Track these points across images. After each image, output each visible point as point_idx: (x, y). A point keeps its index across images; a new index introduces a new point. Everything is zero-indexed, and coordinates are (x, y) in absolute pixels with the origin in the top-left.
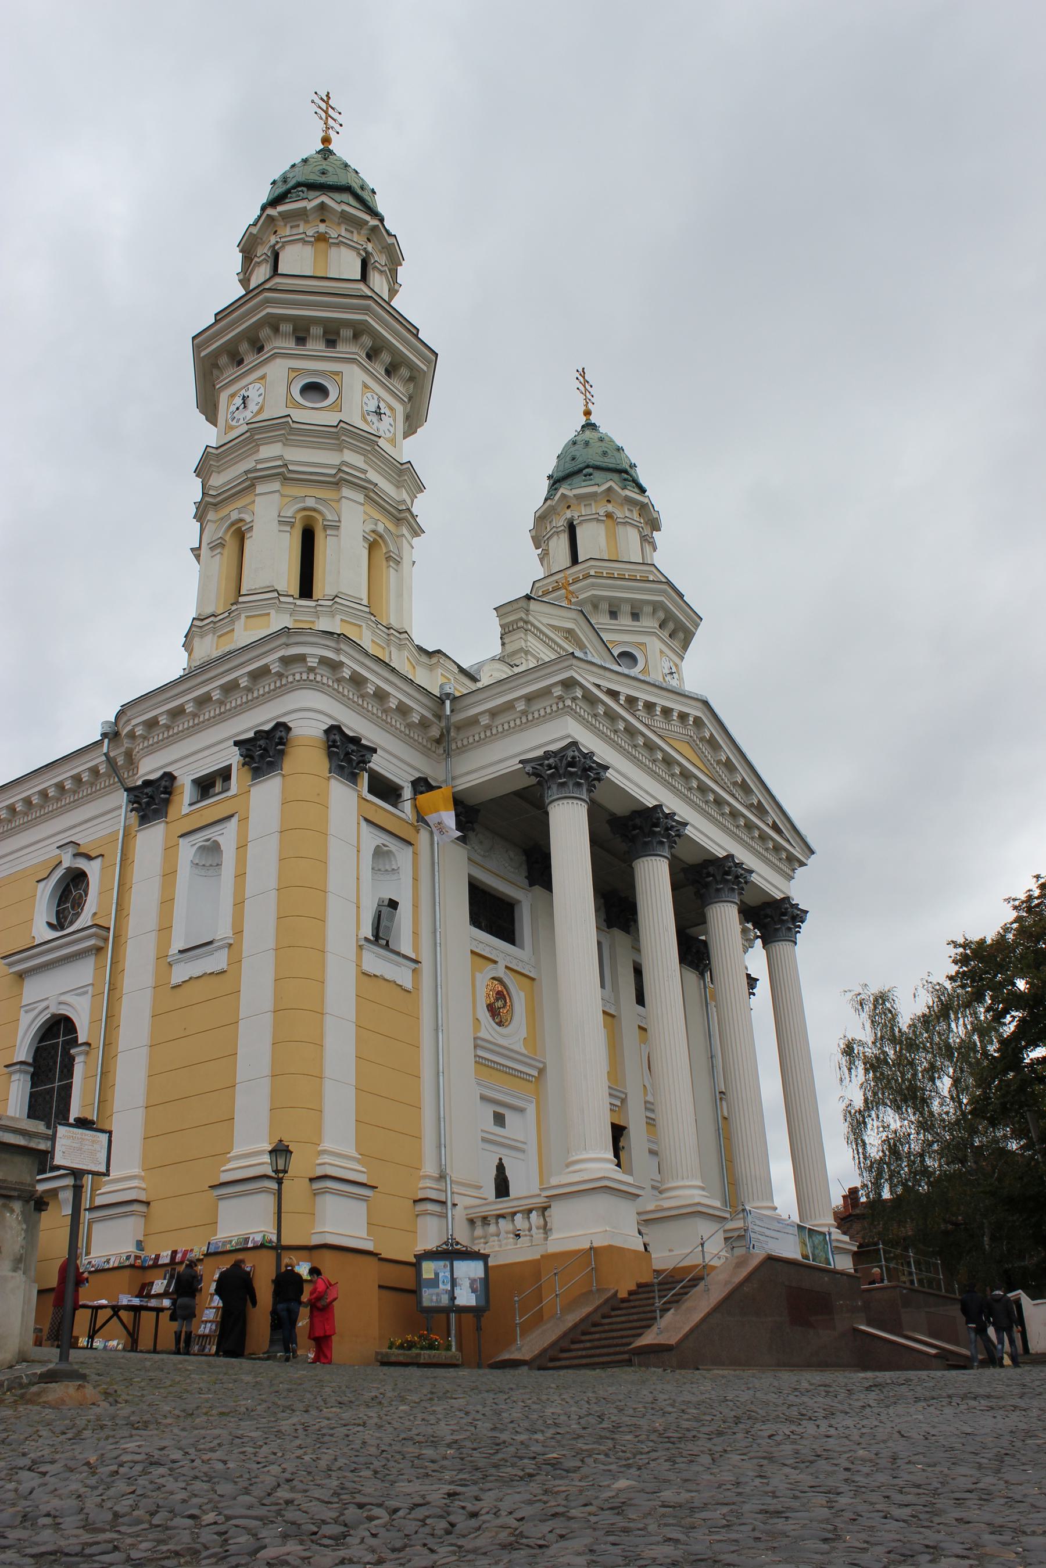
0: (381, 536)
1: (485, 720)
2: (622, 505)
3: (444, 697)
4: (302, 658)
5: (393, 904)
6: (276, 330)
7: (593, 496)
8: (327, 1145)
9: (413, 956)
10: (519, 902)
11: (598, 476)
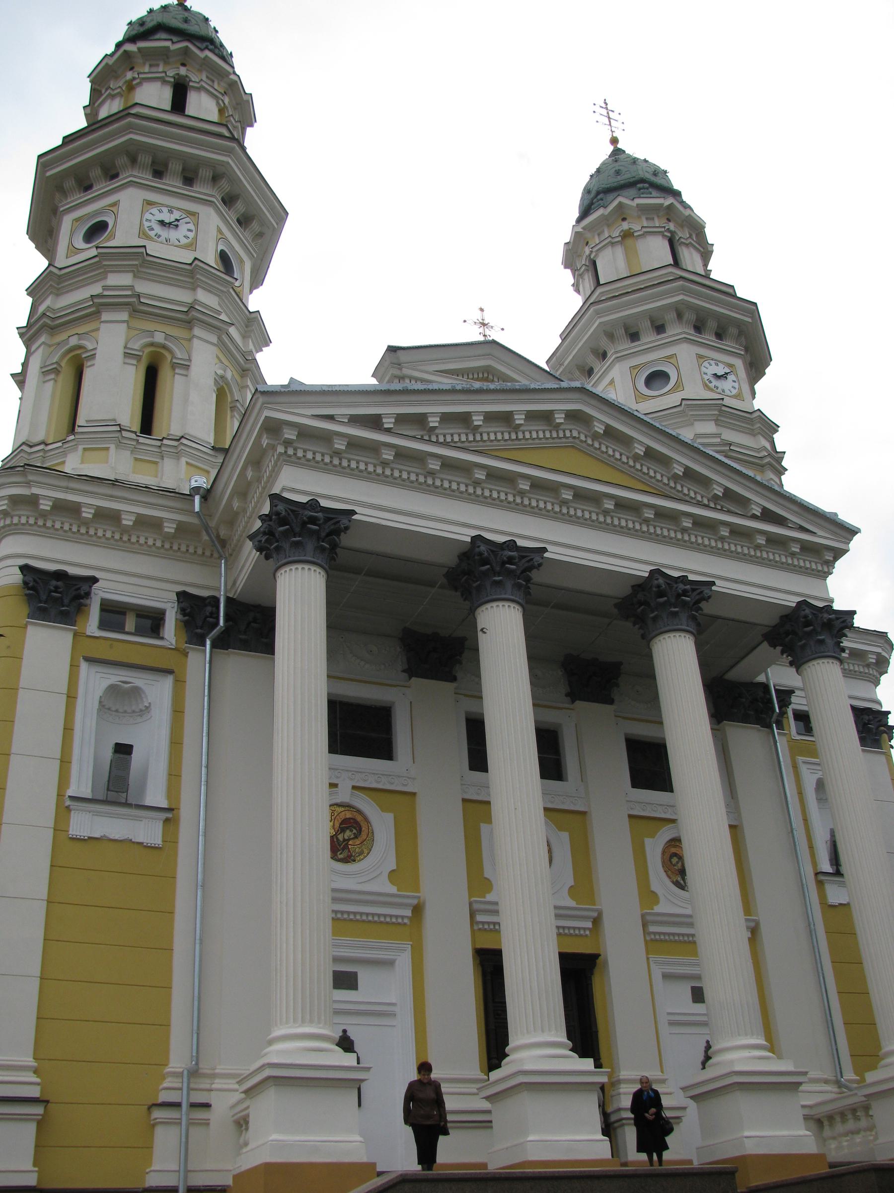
0: (164, 347)
1: (236, 504)
2: (639, 217)
3: (193, 493)
9: (164, 804)
10: (394, 703)
11: (611, 196)
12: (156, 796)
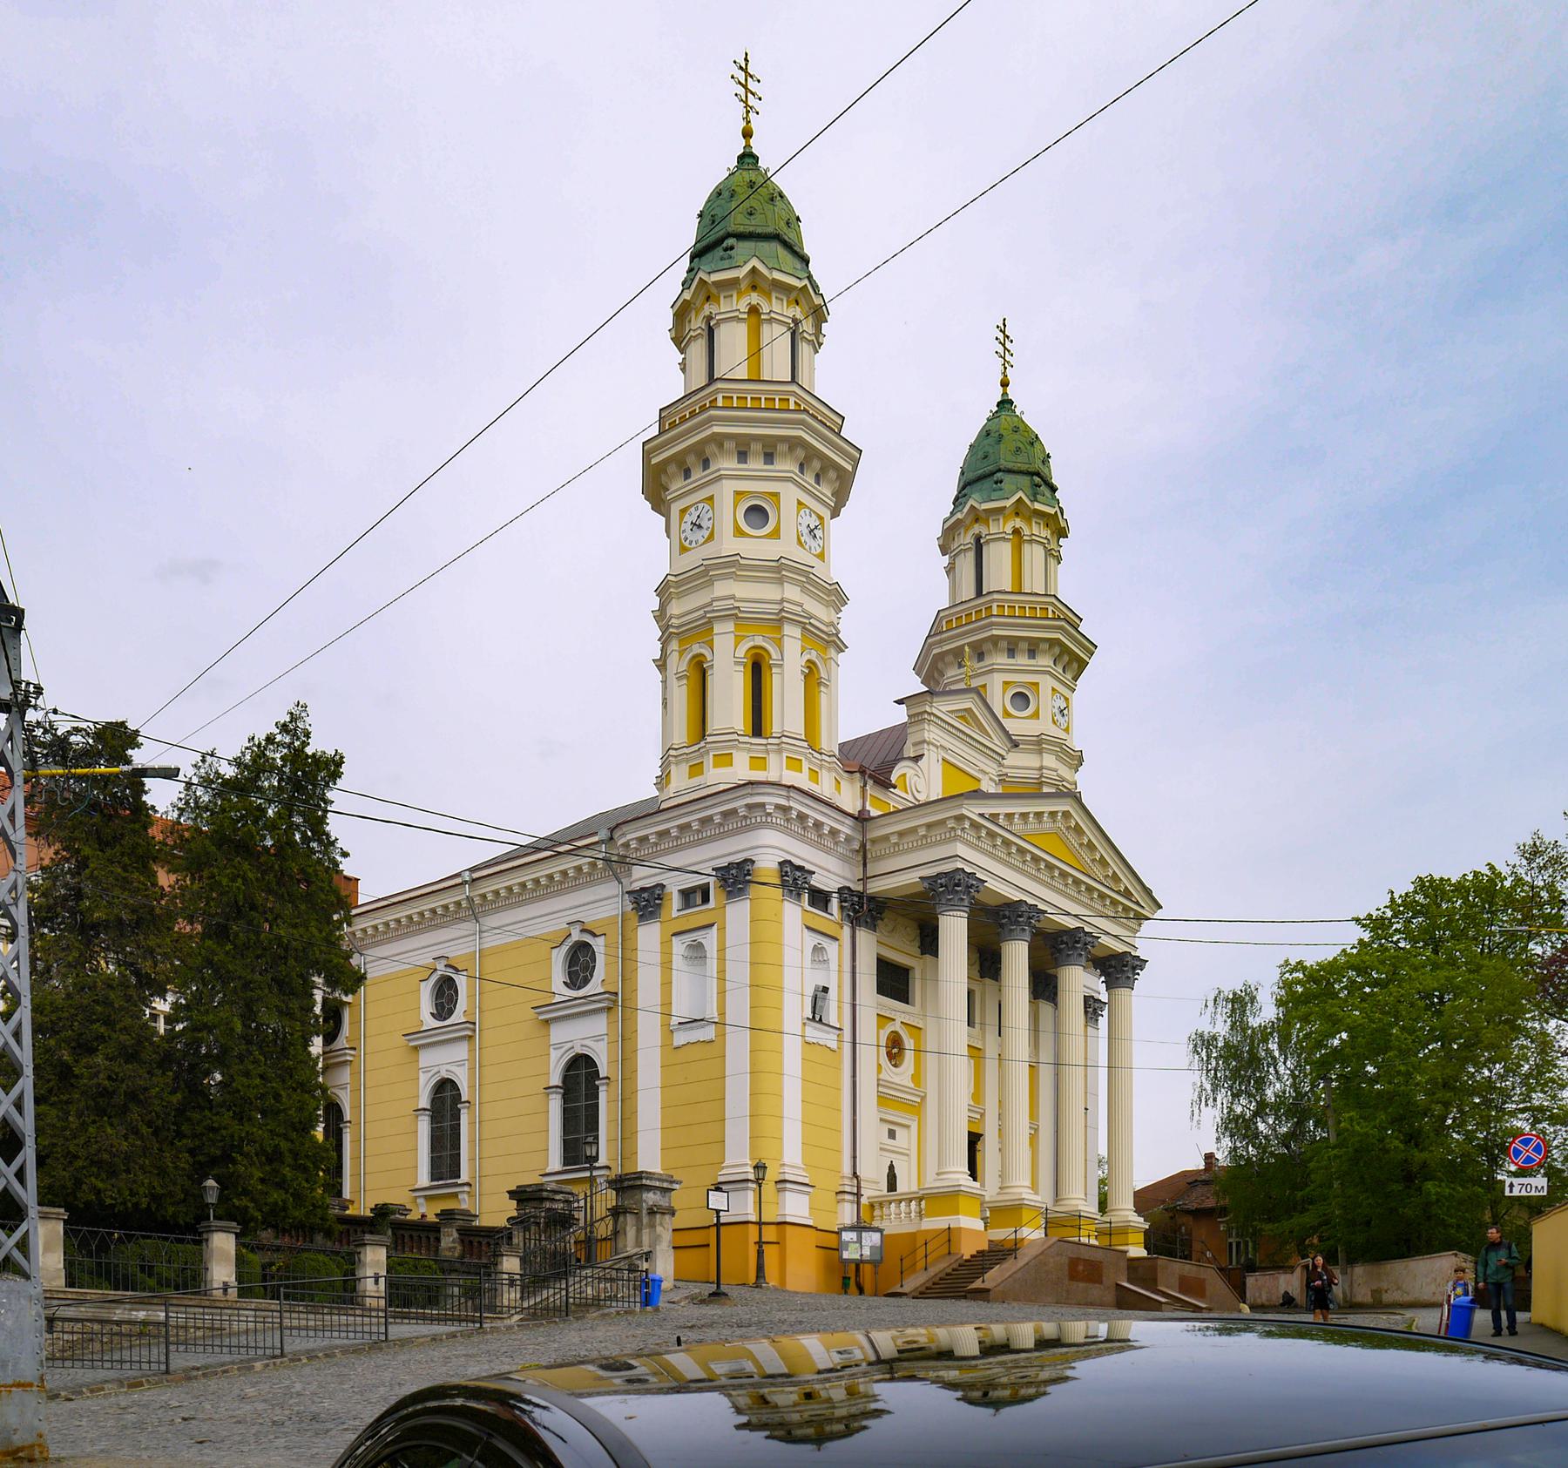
4: (763, 805)
5: (825, 990)
6: (721, 446)
7: (1001, 510)
8: (786, 1160)
12: (832, 1018)
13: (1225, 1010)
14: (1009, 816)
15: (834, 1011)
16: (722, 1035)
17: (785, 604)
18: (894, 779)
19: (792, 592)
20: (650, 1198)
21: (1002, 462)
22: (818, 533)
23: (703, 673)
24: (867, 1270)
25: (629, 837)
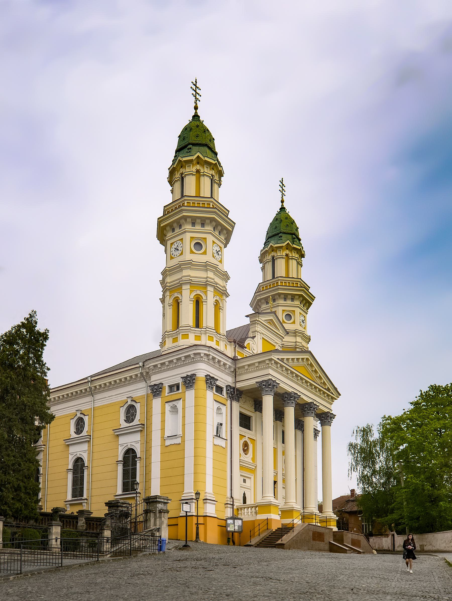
5: (221, 424)
8: (207, 491)
10: (252, 416)
13: (360, 435)
14: (288, 359)
15: (224, 433)
16: (183, 441)
17: (208, 279)
18: (245, 345)
19: (210, 274)
20: (160, 506)
21: (282, 230)
22: (220, 253)
23: (178, 304)
24: (236, 535)
25: (150, 365)
